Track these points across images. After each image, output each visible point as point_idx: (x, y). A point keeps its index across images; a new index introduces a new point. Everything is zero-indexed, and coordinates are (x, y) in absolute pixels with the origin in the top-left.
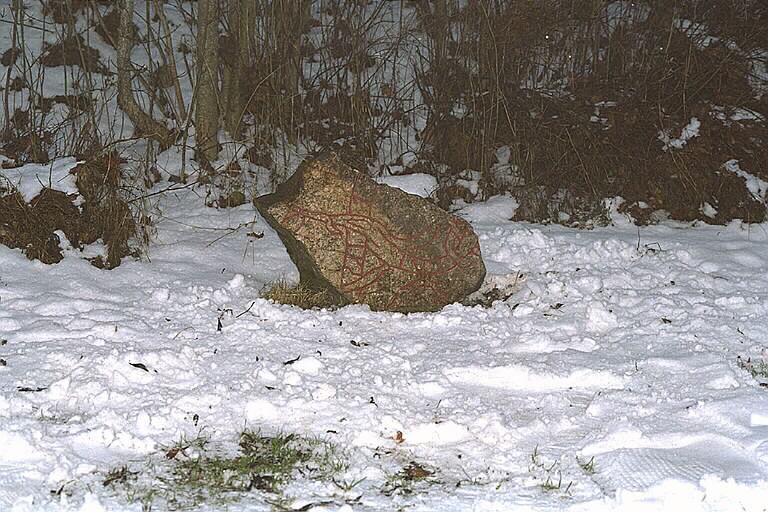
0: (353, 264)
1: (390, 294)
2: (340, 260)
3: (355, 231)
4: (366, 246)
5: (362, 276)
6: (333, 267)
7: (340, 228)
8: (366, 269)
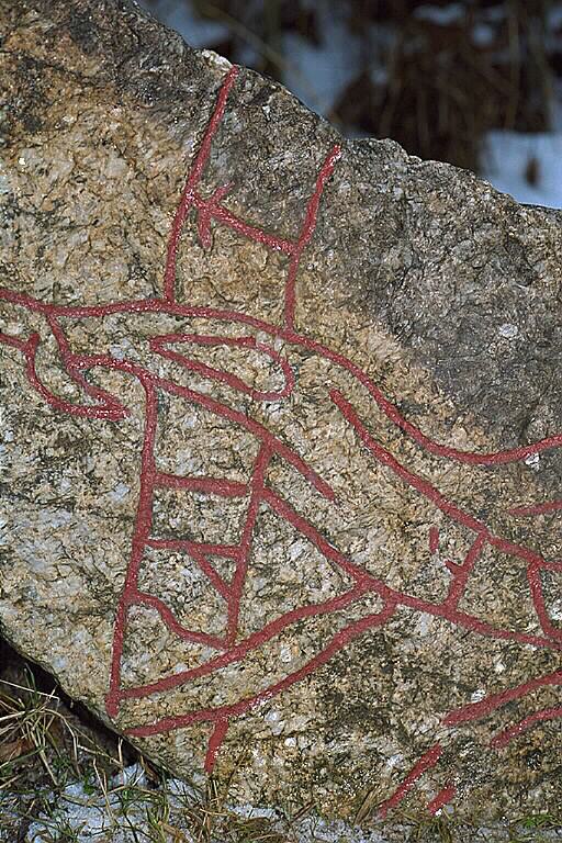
0: (183, 574)
1: (388, 744)
2: (111, 557)
3: (197, 401)
4: (264, 489)
5: (236, 646)
6: (69, 591)
7: (112, 383)
8: (255, 612)
